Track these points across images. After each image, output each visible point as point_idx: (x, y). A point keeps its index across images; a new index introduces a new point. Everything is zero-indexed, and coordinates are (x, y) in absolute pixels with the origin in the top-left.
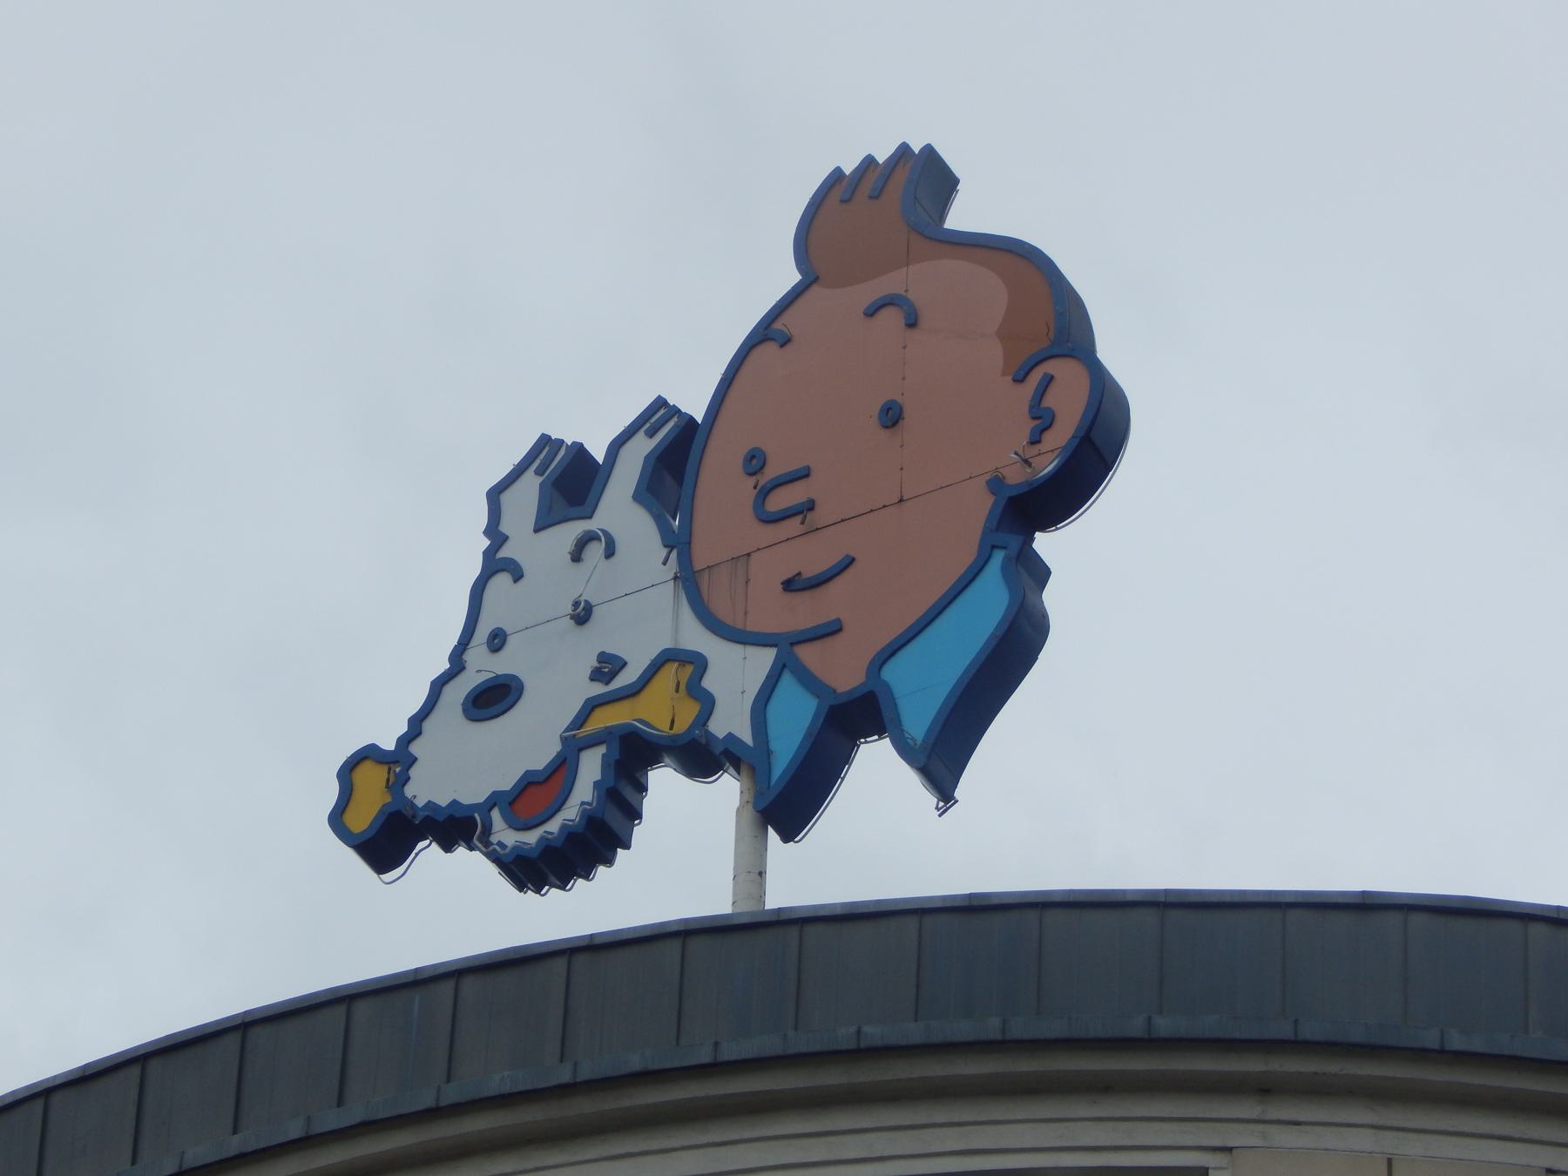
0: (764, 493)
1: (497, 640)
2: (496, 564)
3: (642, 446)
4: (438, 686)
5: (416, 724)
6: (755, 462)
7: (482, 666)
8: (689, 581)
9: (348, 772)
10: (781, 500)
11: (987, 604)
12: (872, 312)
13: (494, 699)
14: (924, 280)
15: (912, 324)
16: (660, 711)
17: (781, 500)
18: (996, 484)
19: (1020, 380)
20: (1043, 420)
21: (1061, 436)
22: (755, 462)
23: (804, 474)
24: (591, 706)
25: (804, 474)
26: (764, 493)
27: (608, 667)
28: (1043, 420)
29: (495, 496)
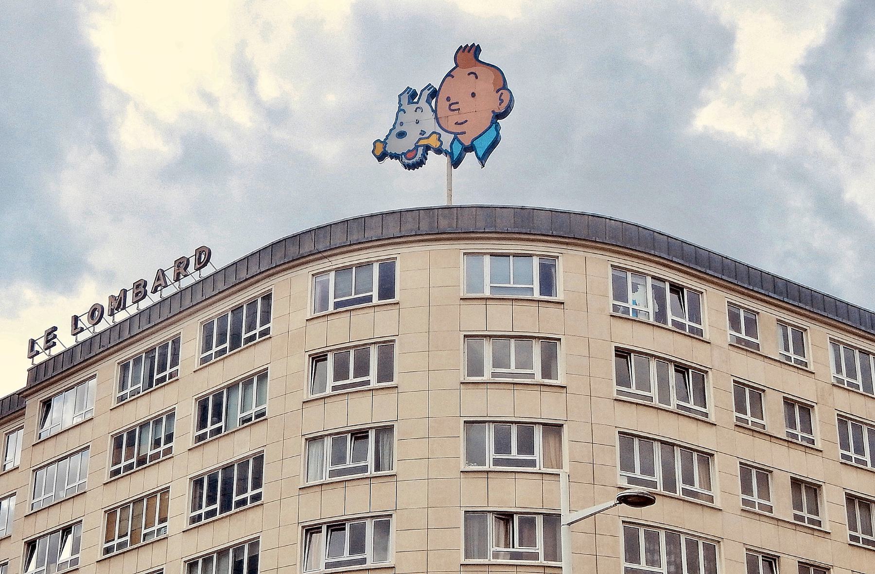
0: (450, 105)
1: (401, 124)
2: (400, 110)
3: (427, 92)
4: (391, 130)
5: (387, 136)
6: (448, 99)
7: (399, 129)
8: (437, 118)
9: (375, 143)
10: (453, 107)
11: (492, 133)
12: (469, 74)
13: (402, 135)
14: (478, 69)
15: (477, 78)
16: (433, 142)
17: (453, 107)
18: (493, 112)
19: (498, 91)
20: (502, 101)
21: (504, 105)
22: (448, 99)
23: (457, 103)
24: (420, 139)
25: (457, 103)
26: (450, 105)
27: (423, 133)
28: (502, 101)
29: (400, 96)
